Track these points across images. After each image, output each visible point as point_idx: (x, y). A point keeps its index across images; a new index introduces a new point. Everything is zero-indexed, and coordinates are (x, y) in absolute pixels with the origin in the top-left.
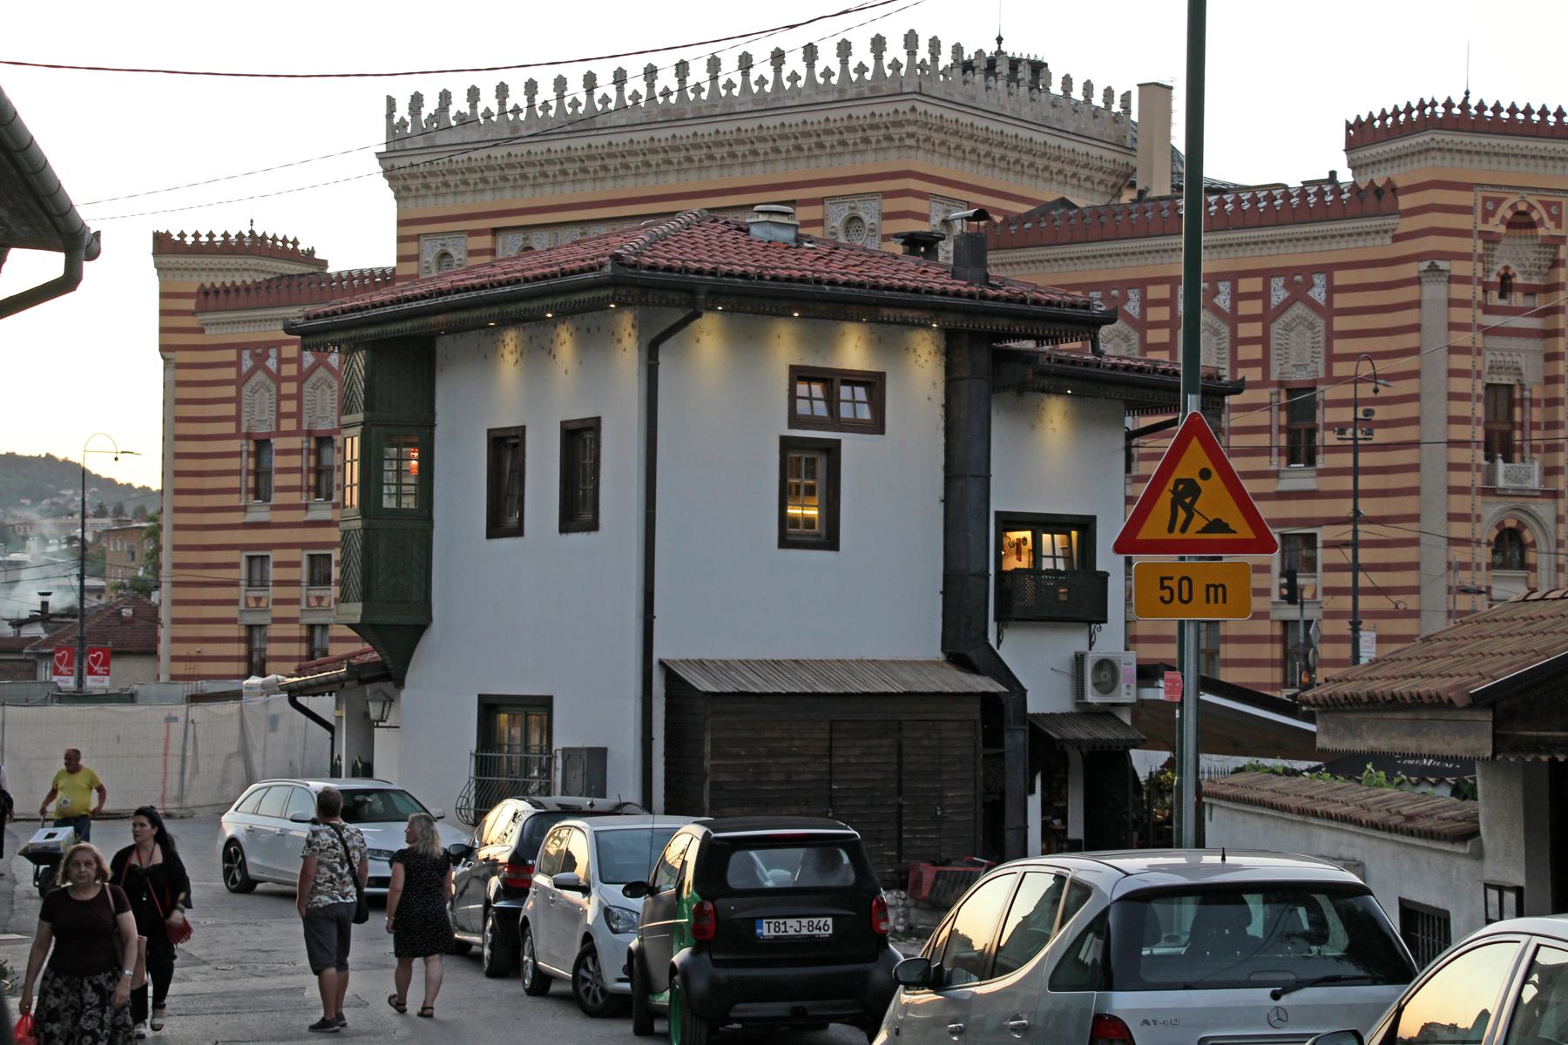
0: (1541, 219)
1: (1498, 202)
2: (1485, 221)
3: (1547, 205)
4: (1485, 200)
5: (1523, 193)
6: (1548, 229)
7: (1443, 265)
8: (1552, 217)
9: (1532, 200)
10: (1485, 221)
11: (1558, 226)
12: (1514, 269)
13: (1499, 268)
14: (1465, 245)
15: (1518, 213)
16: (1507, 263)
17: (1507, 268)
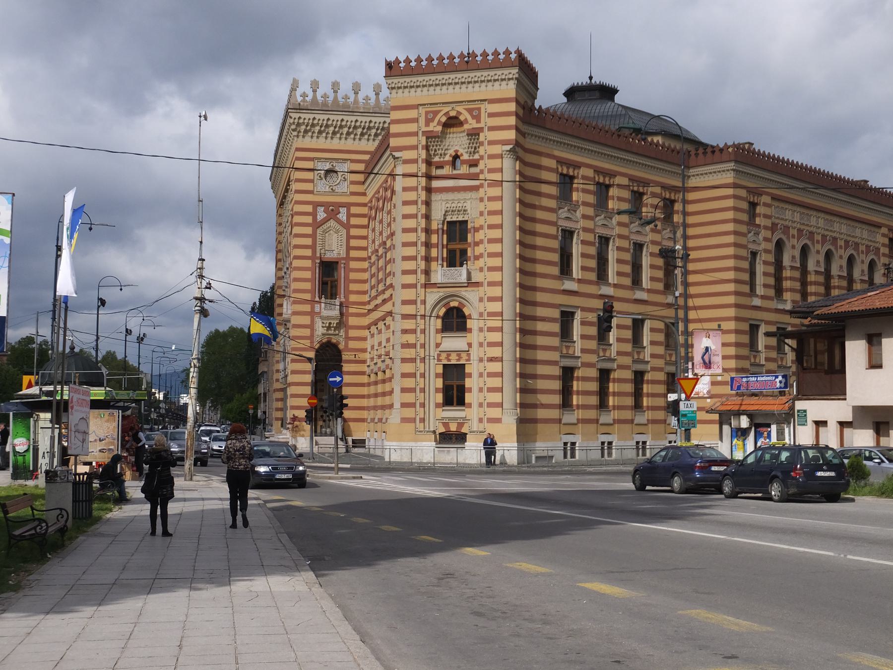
0: (466, 119)
1: (436, 113)
2: (427, 125)
3: (470, 111)
4: (427, 113)
5: (454, 105)
6: (472, 124)
7: (397, 154)
8: (473, 117)
9: (460, 108)
10: (427, 125)
11: (479, 121)
12: (461, 151)
13: (451, 152)
14: (412, 141)
15: (450, 118)
16: (457, 148)
17: (456, 151)
